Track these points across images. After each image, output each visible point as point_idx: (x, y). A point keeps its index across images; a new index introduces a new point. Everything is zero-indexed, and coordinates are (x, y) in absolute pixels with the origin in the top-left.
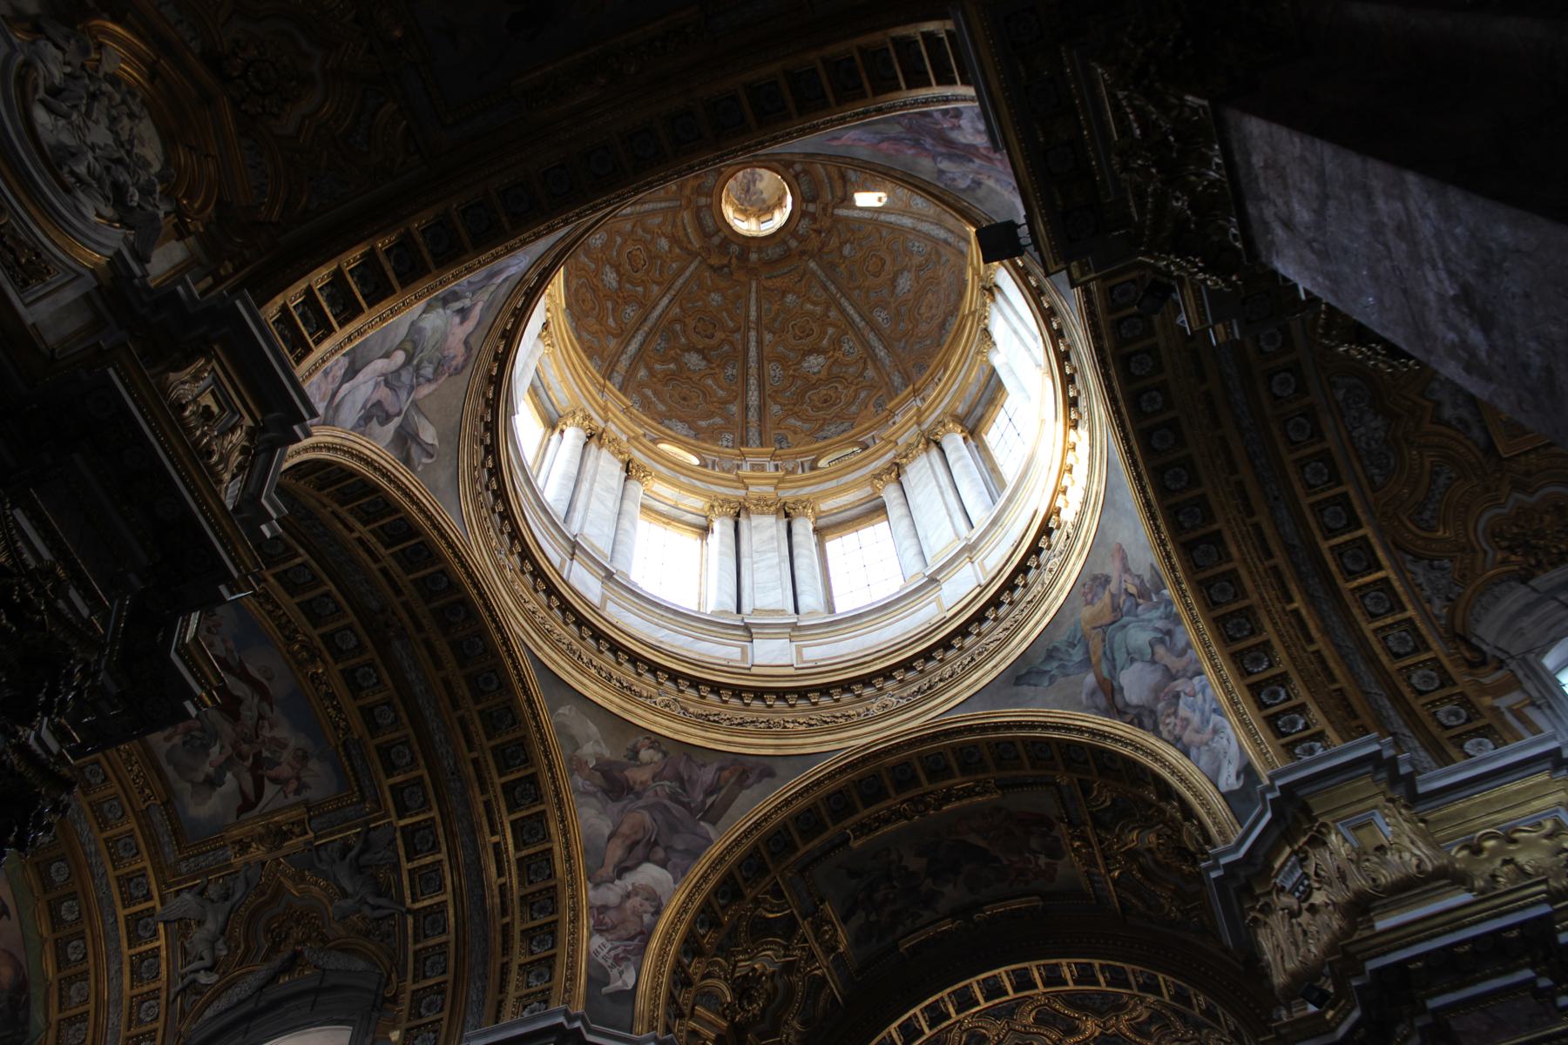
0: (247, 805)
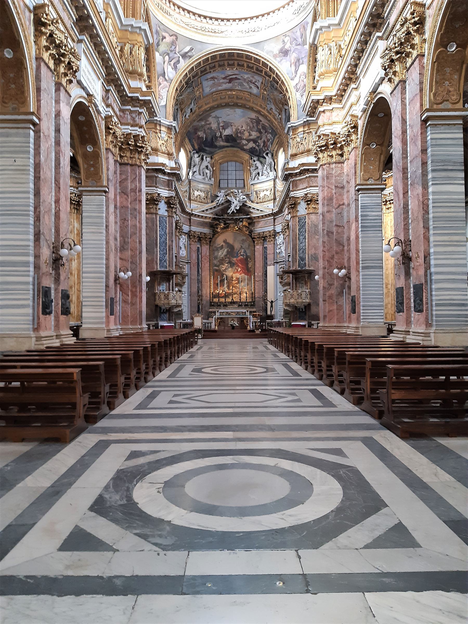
0: (258, 88)
